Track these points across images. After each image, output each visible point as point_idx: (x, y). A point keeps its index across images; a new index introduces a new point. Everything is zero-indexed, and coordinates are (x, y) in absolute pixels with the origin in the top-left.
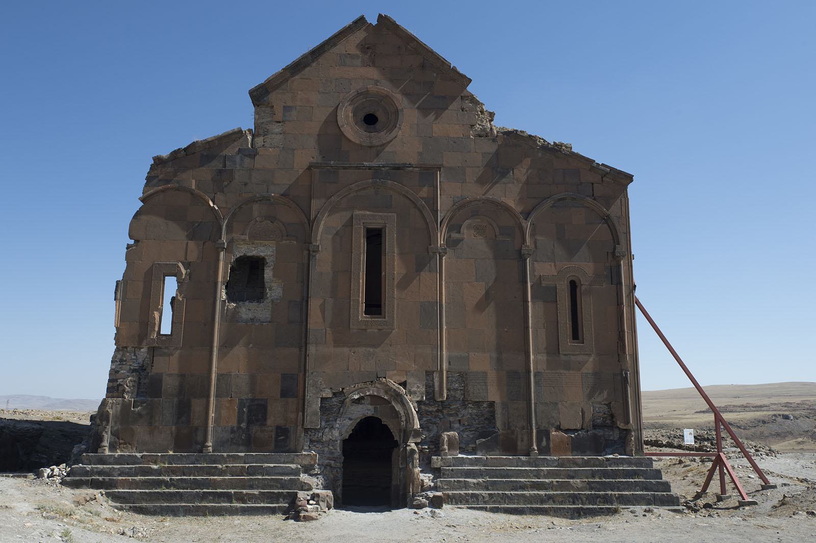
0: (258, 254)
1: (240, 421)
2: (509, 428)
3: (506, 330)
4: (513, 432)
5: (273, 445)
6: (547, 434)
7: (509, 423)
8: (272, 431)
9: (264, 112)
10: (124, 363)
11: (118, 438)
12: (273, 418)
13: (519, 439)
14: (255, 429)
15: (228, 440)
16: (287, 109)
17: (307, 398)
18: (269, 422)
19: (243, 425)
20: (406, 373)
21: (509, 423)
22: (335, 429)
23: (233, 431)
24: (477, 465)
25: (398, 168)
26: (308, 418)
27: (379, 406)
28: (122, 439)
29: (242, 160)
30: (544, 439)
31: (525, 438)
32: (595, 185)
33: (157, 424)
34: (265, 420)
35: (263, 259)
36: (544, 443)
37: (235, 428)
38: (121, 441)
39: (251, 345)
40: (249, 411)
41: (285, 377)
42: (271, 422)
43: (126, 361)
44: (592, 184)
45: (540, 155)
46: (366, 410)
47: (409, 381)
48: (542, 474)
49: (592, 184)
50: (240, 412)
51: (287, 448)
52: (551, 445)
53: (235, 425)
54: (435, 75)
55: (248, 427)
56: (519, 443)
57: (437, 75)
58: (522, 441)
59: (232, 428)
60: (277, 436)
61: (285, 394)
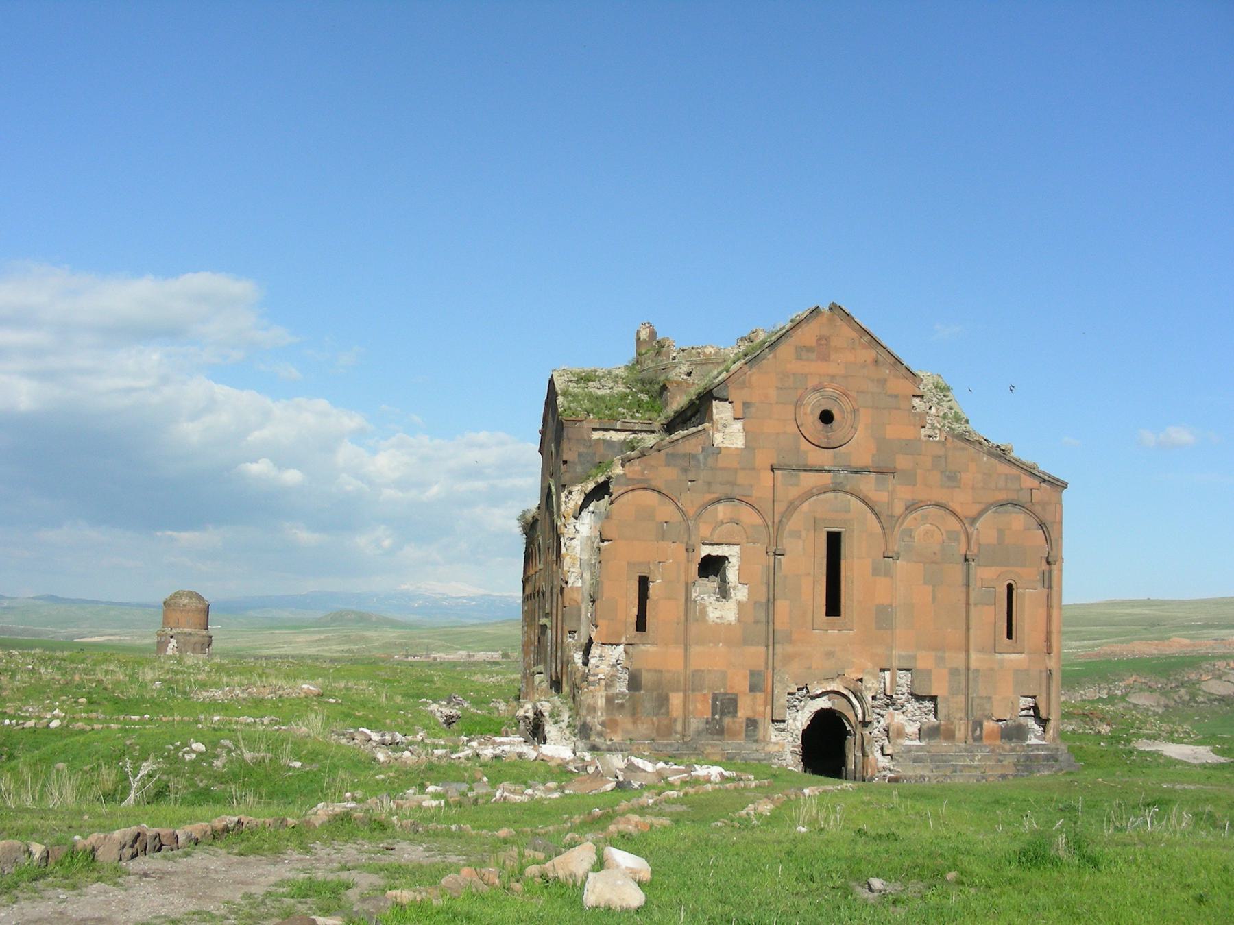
0: (723, 555)
1: (713, 715)
2: (949, 720)
3: (949, 630)
4: (952, 724)
5: (743, 734)
6: (981, 725)
7: (949, 715)
8: (742, 722)
9: (723, 406)
10: (603, 658)
11: (605, 727)
12: (743, 711)
13: (957, 728)
14: (727, 720)
15: (703, 731)
16: (746, 405)
17: (776, 693)
18: (740, 714)
19: (717, 717)
20: (863, 670)
21: (949, 715)
22: (797, 721)
23: (707, 723)
24: (922, 752)
25: (856, 472)
26: (777, 711)
27: (836, 700)
28: (609, 728)
29: (705, 458)
30: (978, 729)
31: (963, 728)
32: (1033, 491)
33: (639, 715)
34: (736, 712)
35: (726, 558)
36: (978, 732)
37: (710, 720)
38: (608, 731)
39: (721, 645)
40: (721, 704)
41: (752, 673)
42: (743, 713)
43: (604, 657)
44: (1031, 489)
45: (985, 459)
46: (823, 703)
47: (865, 678)
48: (976, 758)
49: (1031, 489)
50: (714, 706)
51: (756, 737)
52: (984, 733)
53: (710, 716)
54: (888, 371)
55: (721, 718)
56: (957, 732)
57: (890, 372)
58: (960, 730)
59: (707, 719)
60: (747, 726)
61: (753, 689)
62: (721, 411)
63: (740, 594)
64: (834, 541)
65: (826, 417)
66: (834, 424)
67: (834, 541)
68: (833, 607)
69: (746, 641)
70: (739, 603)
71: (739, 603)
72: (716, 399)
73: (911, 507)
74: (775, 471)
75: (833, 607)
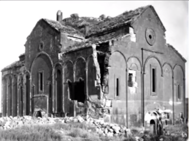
61: (139, 113)
62: (131, 30)
63: (135, 84)
64: (154, 70)
65: (150, 37)
66: (152, 39)
67: (154, 70)
68: (154, 90)
69: (137, 99)
70: (136, 88)
71: (136, 88)
72: (131, 27)
73: (165, 64)
74: (144, 51)
75: (154, 90)
